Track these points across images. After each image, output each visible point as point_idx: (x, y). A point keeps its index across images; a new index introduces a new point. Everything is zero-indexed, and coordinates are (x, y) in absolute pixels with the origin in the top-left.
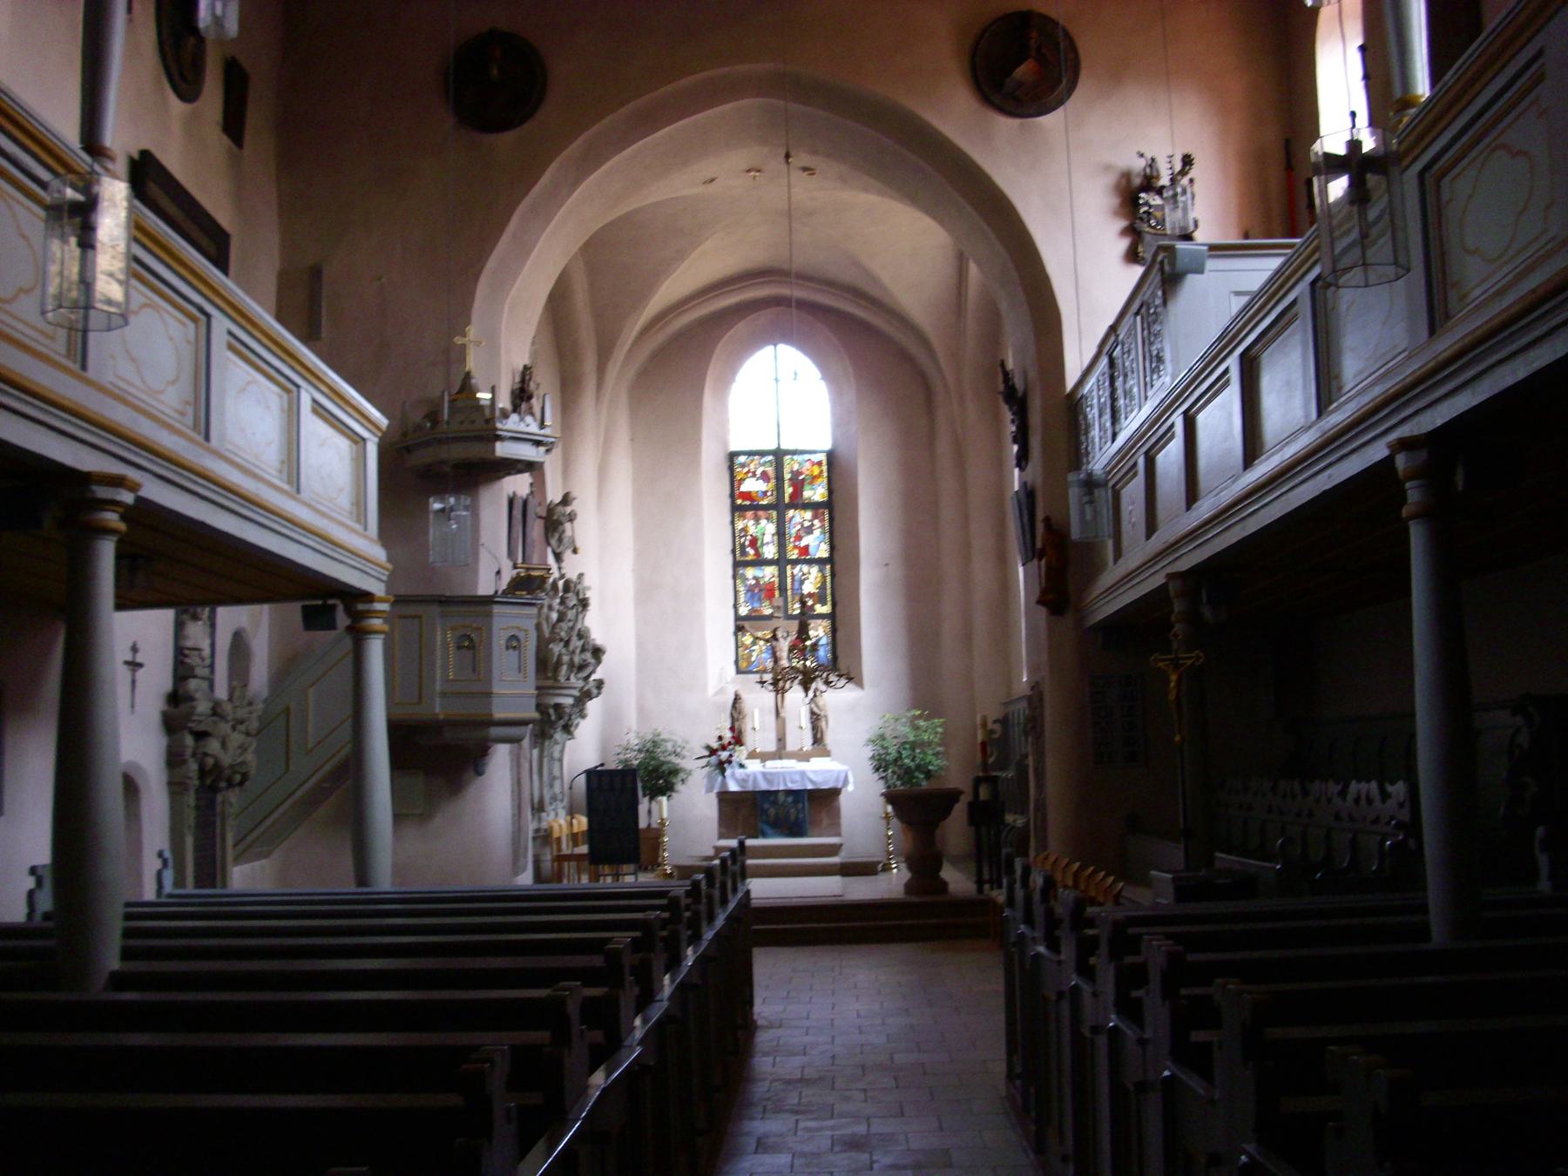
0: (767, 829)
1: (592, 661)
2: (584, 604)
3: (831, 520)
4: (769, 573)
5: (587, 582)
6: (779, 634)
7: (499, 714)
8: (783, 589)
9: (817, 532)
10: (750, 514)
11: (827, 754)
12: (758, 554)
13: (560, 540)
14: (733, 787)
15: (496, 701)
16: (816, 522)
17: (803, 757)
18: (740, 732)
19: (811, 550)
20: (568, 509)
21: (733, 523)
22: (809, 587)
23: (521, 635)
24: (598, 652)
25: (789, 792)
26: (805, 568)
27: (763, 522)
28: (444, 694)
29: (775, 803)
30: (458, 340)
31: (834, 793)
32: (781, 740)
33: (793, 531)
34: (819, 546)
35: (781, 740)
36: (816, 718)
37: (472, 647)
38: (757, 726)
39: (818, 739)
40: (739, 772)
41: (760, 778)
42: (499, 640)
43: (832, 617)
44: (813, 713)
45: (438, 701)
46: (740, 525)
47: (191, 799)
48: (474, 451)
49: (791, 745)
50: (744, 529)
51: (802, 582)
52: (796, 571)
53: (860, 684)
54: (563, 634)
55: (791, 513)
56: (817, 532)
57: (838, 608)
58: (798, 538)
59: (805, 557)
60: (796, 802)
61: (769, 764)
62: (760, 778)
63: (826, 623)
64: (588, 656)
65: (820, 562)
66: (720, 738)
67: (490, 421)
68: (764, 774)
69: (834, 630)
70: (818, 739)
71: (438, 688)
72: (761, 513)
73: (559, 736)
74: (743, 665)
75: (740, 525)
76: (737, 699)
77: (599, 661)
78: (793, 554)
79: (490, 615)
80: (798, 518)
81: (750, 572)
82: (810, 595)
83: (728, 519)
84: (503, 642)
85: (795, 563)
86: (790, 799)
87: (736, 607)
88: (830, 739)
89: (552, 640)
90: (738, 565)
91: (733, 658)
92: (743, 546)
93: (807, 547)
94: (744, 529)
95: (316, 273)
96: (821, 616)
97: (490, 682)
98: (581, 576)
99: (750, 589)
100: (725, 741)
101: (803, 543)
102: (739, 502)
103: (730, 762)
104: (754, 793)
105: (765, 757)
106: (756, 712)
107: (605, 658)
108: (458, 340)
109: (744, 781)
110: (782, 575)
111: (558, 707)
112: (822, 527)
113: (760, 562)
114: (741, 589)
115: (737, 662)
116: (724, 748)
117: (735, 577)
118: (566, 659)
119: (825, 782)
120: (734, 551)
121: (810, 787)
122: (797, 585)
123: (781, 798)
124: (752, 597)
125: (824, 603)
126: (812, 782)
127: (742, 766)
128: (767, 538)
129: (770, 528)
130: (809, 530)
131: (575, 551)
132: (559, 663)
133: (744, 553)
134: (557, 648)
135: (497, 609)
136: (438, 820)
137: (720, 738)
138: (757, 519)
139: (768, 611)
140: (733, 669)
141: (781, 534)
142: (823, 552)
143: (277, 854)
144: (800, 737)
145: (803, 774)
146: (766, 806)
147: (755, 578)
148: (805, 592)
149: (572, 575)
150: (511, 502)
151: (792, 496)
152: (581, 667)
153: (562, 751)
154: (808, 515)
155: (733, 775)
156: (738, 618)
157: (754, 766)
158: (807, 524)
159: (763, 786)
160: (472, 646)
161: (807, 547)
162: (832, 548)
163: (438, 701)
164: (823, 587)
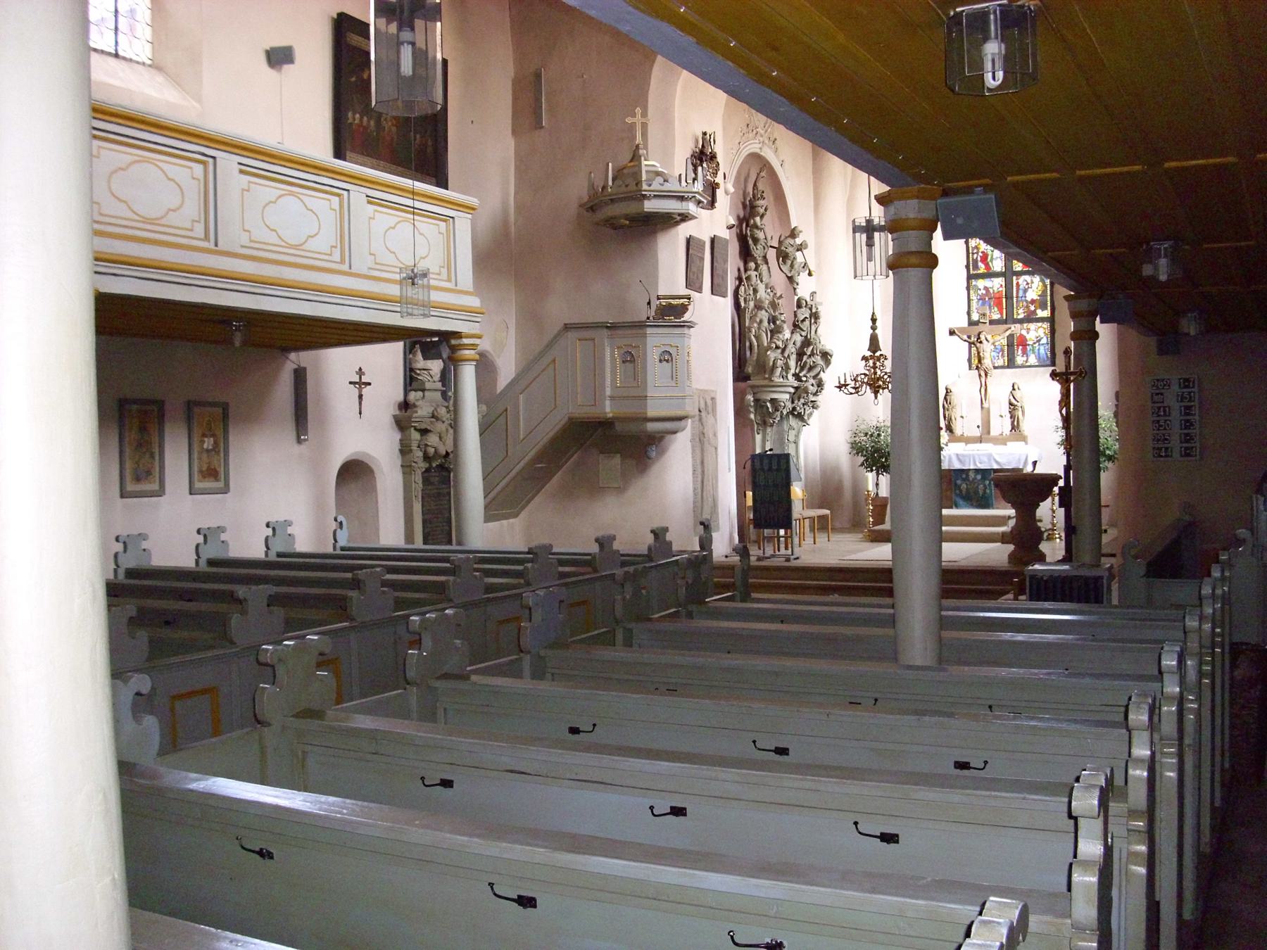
0: (961, 502)
1: (822, 363)
2: (815, 316)
4: (997, 284)
5: (818, 298)
6: (982, 337)
7: (651, 413)
8: (1009, 297)
11: (1023, 439)
13: (792, 266)
15: (649, 402)
17: (1001, 440)
20: (798, 241)
22: (1033, 294)
23: (673, 351)
24: (826, 356)
25: (977, 471)
26: (1028, 278)
28: (612, 398)
29: (967, 479)
30: (629, 120)
37: (633, 361)
39: (1015, 427)
42: (653, 355)
44: (1011, 404)
45: (608, 403)
47: (418, 478)
48: (631, 208)
49: (994, 432)
50: (976, 247)
51: (1025, 291)
54: (780, 344)
60: (984, 478)
63: (1046, 325)
64: (818, 359)
67: (639, 183)
69: (1053, 332)
70: (1015, 427)
71: (608, 392)
73: (793, 422)
77: (828, 363)
79: (645, 336)
81: (981, 283)
82: (1033, 302)
84: (657, 358)
86: (979, 477)
87: (969, 314)
88: (1025, 426)
89: (769, 348)
90: (970, 277)
92: (975, 262)
95: (538, 76)
96: (1042, 320)
97: (645, 388)
98: (813, 294)
99: (982, 299)
104: (950, 470)
105: (968, 440)
107: (833, 360)
108: (629, 120)
110: (1009, 285)
111: (773, 401)
113: (990, 275)
114: (973, 297)
117: (968, 289)
118: (780, 363)
119: (1009, 463)
120: (967, 267)
121: (996, 467)
122: (1021, 294)
123: (972, 475)
124: (983, 304)
125: (1043, 307)
126: (997, 463)
131: (810, 274)
132: (774, 367)
134: (772, 355)
135: (649, 331)
136: (631, 492)
139: (996, 316)
143: (523, 514)
144: (1001, 425)
146: (959, 482)
147: (986, 288)
148: (1029, 299)
149: (803, 291)
150: (689, 241)
152: (811, 369)
153: (797, 436)
159: (957, 466)
160: (631, 359)
163: (608, 403)
164: (1043, 295)
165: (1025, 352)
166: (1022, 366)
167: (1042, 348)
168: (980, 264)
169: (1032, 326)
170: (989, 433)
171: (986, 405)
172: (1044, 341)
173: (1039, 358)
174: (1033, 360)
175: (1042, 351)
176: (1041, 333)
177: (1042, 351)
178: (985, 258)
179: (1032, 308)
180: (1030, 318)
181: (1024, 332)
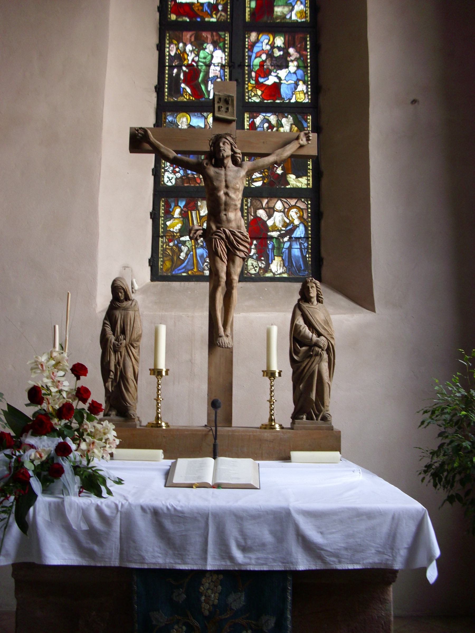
3: (316, 49)
9: (293, 67)
10: (188, 35)
12: (197, 92)
14: (57, 553)
16: (291, 50)
18: (123, 377)
19: (284, 91)
21: (161, 48)
26: (273, 119)
27: (210, 47)
31: (376, 579)
32: (220, 403)
33: (257, 62)
34: (292, 83)
35: (220, 403)
36: (306, 351)
38: (162, 365)
39: (309, 399)
40: (78, 502)
41: (143, 526)
43: (314, 195)
44: (297, 338)
46: (172, 50)
52: (258, 121)
53: (362, 298)
55: (253, 36)
56: (293, 67)
57: (324, 182)
58: (264, 72)
59: (273, 101)
61: (185, 467)
62: (143, 526)
65: (296, 110)
66: (35, 395)
68: (156, 515)
69: (316, 219)
70: (309, 399)
72: (206, 35)
74: (165, 265)
75: (172, 50)
76: (119, 294)
78: (255, 97)
80: (264, 44)
83: (154, 39)
85: (256, 109)
86: (237, 601)
91: (148, 254)
92: (175, 82)
93: (276, 87)
94: (180, 57)
96: (297, 193)
100: (52, 404)
101: (271, 80)
102: (173, 17)
103: (50, 472)
104: (123, 573)
106: (163, 330)
109: (87, 537)
112: (301, 59)
115: (153, 263)
116: (41, 425)
119: (356, 550)
120: (159, 89)
121: (303, 563)
123: (210, 595)
127: (93, 483)
128: (214, 71)
129: (219, 57)
130: (282, 63)
133: (175, 89)
137: (35, 395)
138: (199, 45)
140: (148, 270)
141: (236, 65)
142: (301, 95)
144: (263, 397)
145: (282, 520)
151: (253, 14)
154: (279, 41)
155: (59, 512)
156: (161, 193)
157: (137, 480)
158: (277, 53)
159: (154, 555)
161: (276, 87)
162: (316, 89)
165: (262, 253)
166: (258, 278)
167: (296, 246)
168: (183, 85)
169: (279, 205)
170: (228, 420)
171: (225, 340)
172: (300, 232)
173: (288, 262)
174: (277, 267)
175: (296, 252)
176: (293, 213)
177: (296, 252)
178: (193, 75)
179: (279, 171)
180: (275, 188)
181: (262, 213)
